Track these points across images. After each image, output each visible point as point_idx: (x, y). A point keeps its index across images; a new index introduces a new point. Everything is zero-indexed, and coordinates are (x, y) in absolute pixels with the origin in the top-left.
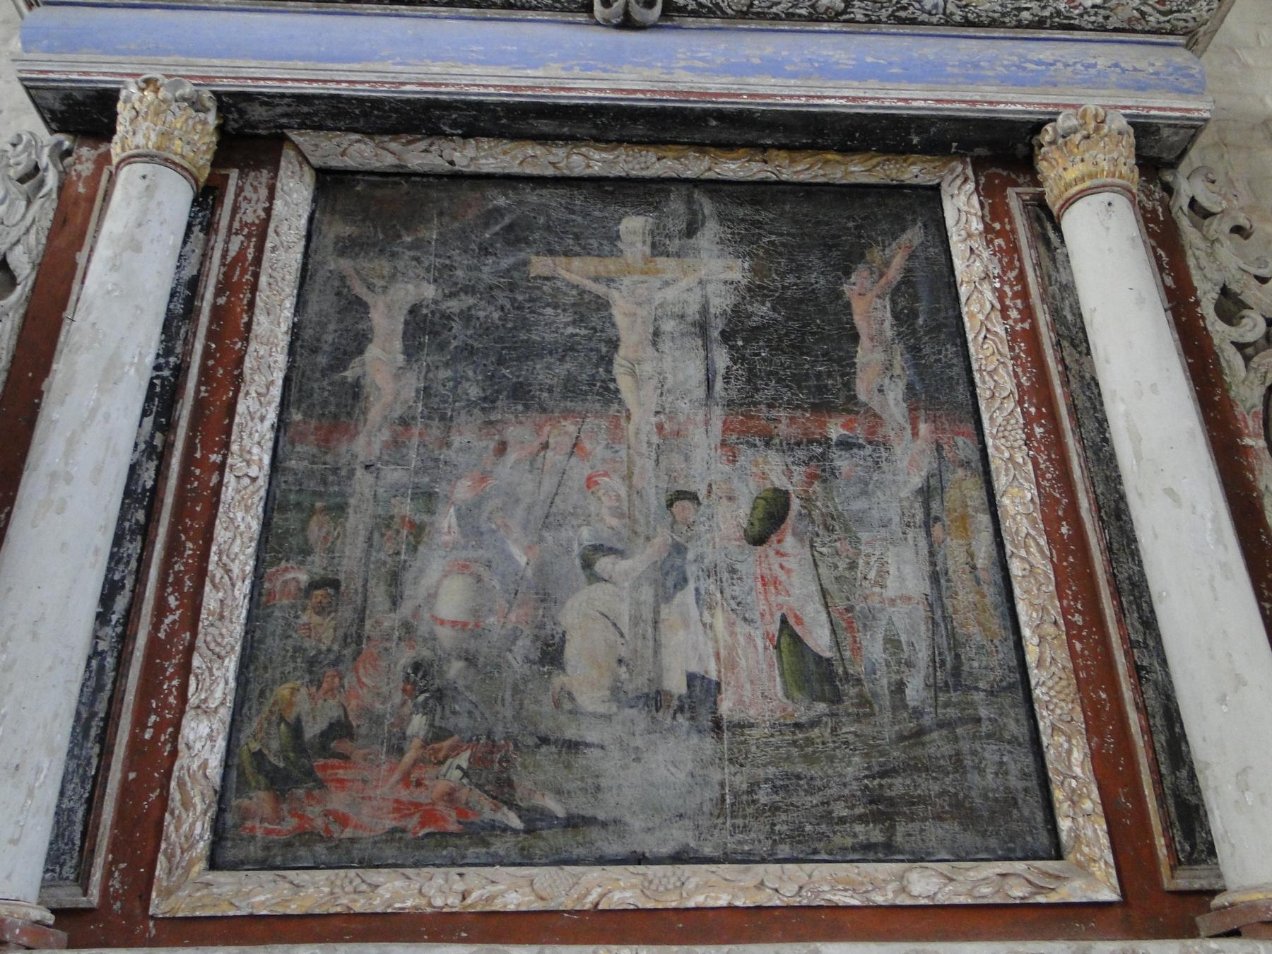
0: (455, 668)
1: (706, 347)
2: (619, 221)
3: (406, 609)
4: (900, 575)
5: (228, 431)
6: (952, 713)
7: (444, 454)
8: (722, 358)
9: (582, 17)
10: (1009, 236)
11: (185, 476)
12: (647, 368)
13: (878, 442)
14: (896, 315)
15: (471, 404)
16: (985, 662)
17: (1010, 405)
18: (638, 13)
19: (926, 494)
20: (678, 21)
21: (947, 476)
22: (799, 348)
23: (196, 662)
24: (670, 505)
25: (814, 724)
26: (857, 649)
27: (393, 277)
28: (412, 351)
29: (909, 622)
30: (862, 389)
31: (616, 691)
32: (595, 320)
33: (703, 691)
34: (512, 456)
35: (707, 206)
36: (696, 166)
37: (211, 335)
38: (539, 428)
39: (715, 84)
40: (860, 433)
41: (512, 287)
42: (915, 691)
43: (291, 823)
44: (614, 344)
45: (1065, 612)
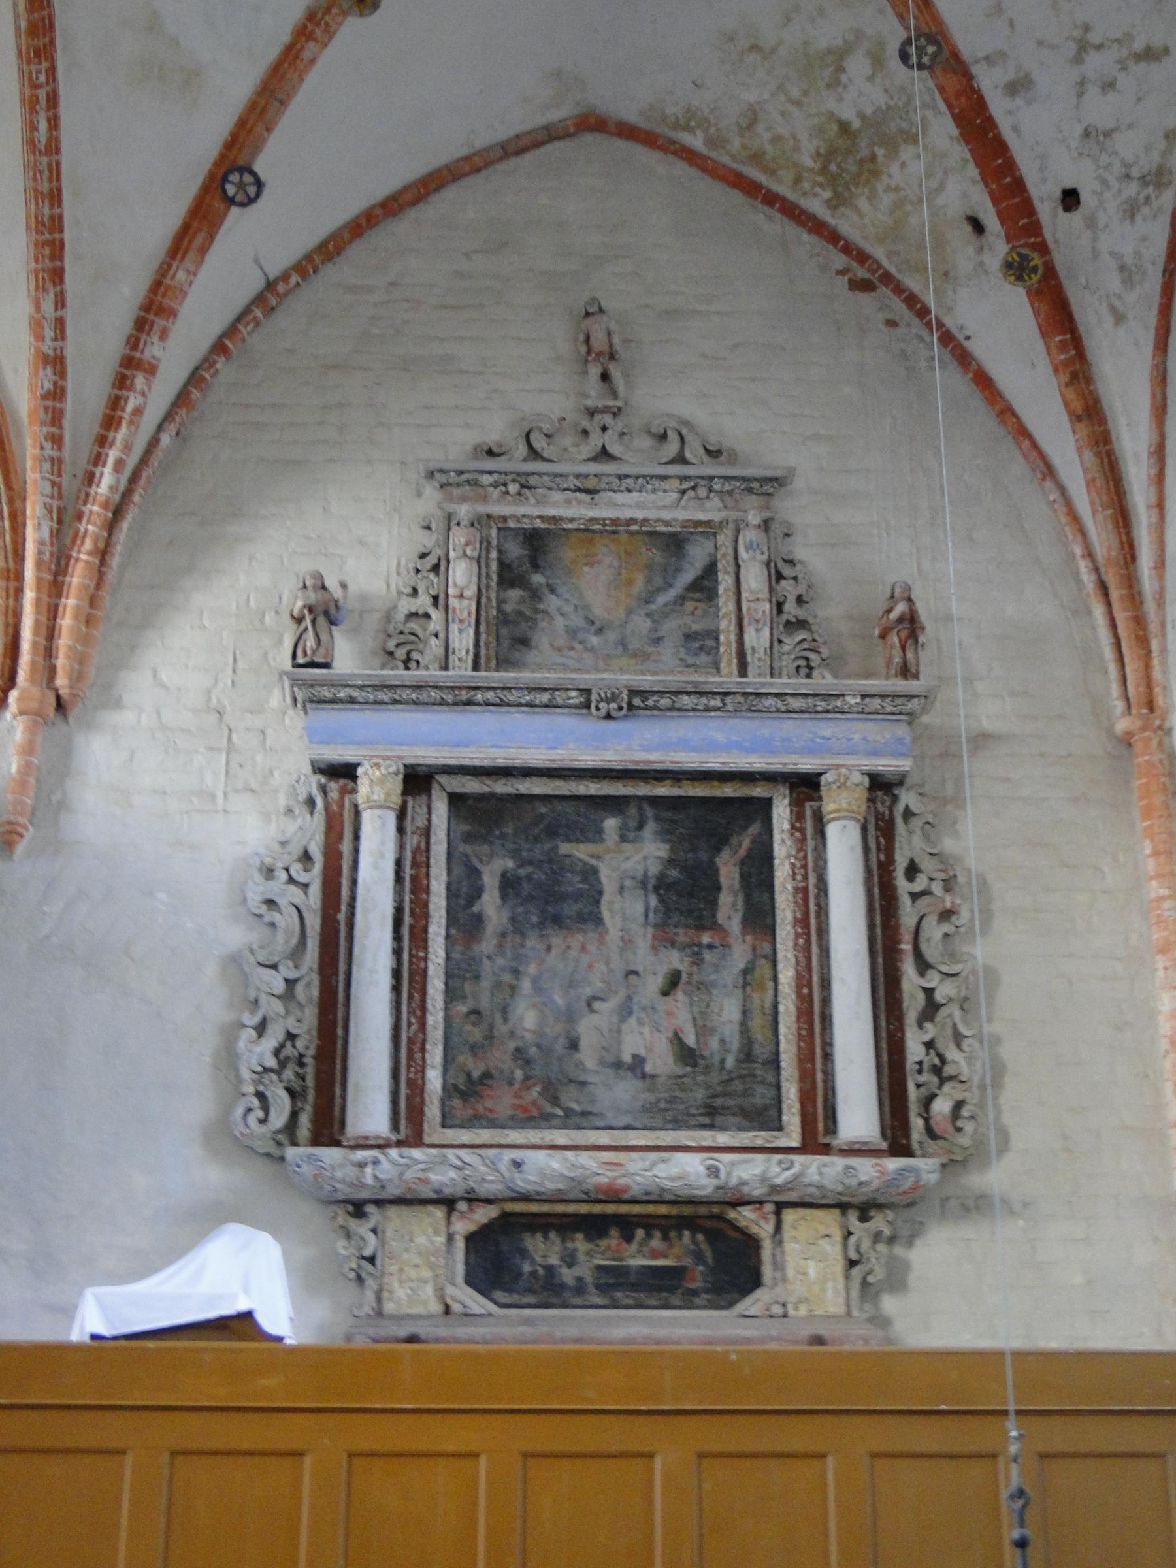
0: (533, 1051)
1: (646, 896)
2: (602, 821)
3: (510, 1024)
4: (728, 1011)
5: (426, 940)
6: (745, 1072)
7: (522, 951)
8: (653, 901)
9: (585, 711)
10: (802, 830)
11: (411, 963)
12: (617, 907)
13: (725, 946)
14: (742, 876)
15: (533, 926)
16: (761, 1051)
17: (789, 928)
18: (614, 714)
19: (746, 972)
20: (635, 712)
21: (758, 963)
22: (691, 895)
23: (428, 1047)
24: (626, 976)
25: (684, 1076)
26: (706, 1044)
27: (492, 856)
28: (504, 897)
30: (721, 917)
31: (602, 1062)
32: (591, 878)
33: (638, 1061)
34: (554, 952)
35: (649, 812)
36: (644, 790)
37: (412, 892)
38: (565, 937)
39: (652, 757)
40: (717, 943)
41: (550, 861)
42: (730, 1063)
43: (471, 1112)
44: (601, 893)
45: (799, 1029)
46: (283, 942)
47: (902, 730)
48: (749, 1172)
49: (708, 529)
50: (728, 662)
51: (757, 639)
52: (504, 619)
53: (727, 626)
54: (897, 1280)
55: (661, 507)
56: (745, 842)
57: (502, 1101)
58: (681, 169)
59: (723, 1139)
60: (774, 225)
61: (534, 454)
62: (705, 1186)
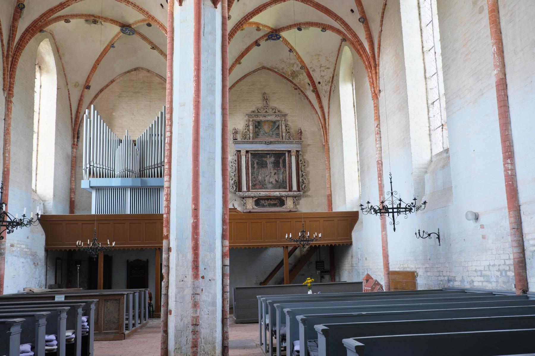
4: (281, 176)
29: (281, 179)
46: (234, 170)
47: (300, 145)
48: (283, 194)
49: (278, 121)
50: (281, 137)
52: (256, 132)
53: (281, 132)
54: (298, 204)
55: (272, 118)
57: (258, 187)
58: (275, 74)
60: (285, 81)
61: (258, 112)
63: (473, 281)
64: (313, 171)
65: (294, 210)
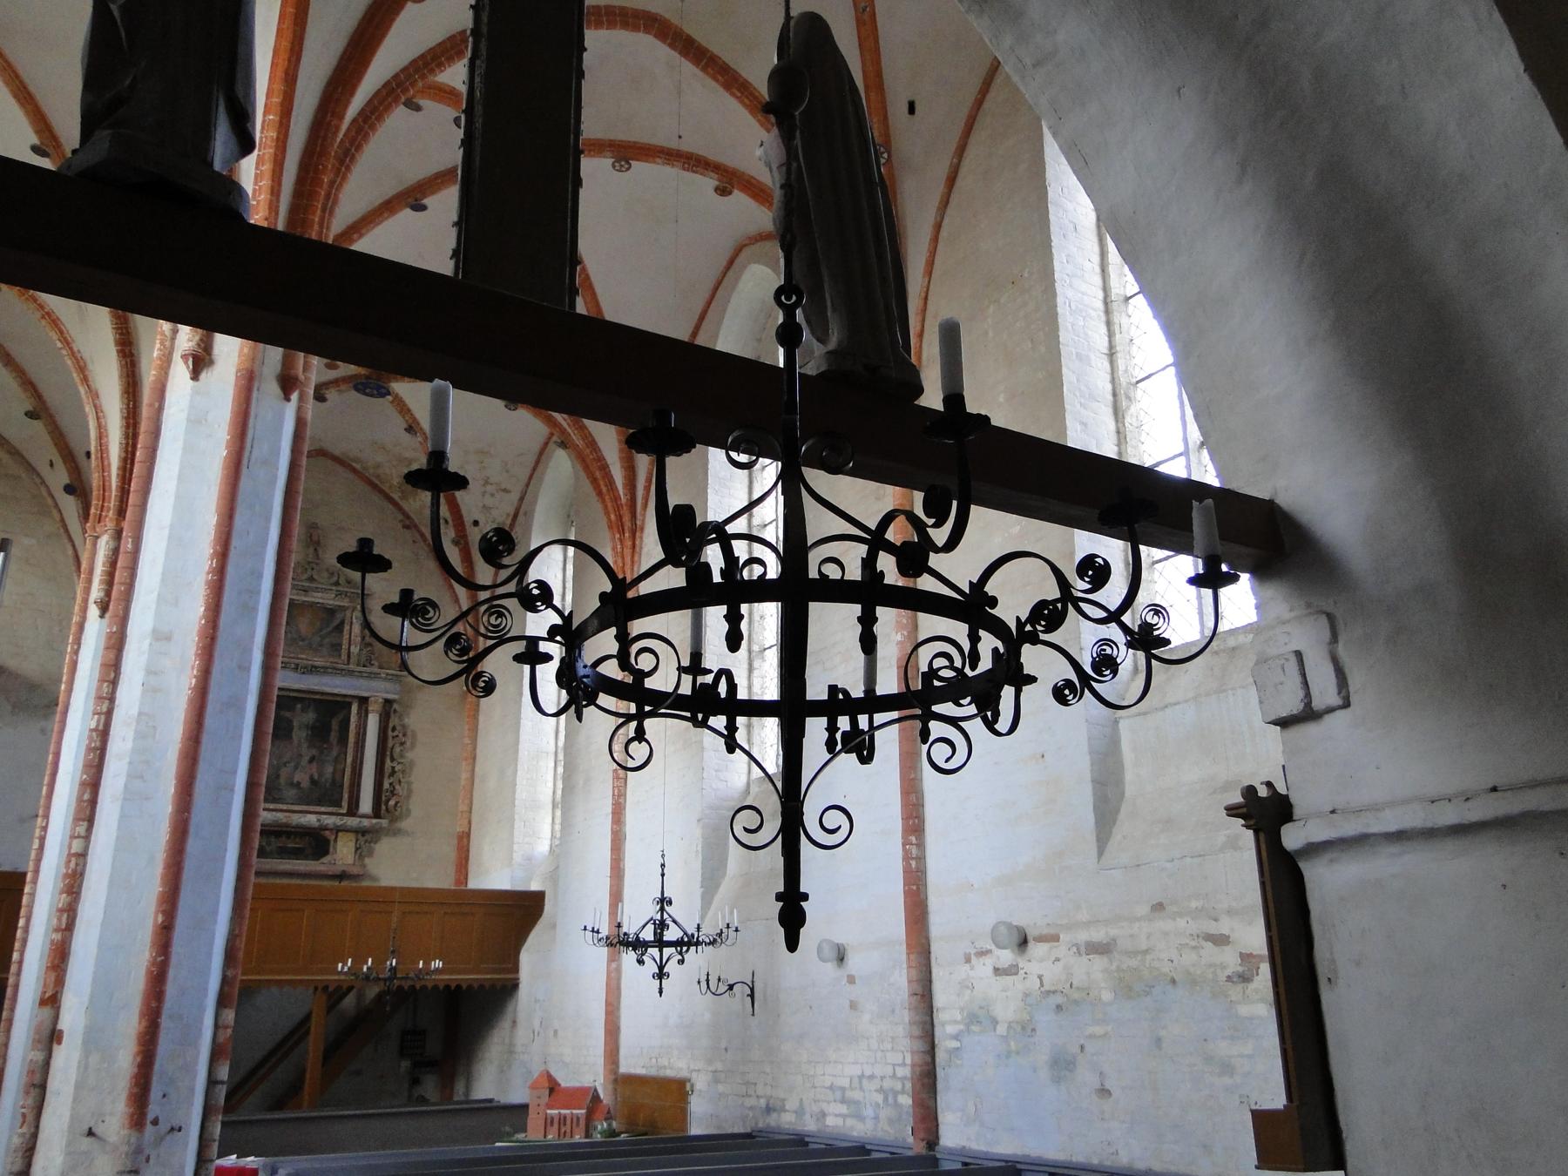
4: (329, 769)
33: (299, 783)
47: (398, 687)
48: (330, 821)
49: (343, 609)
50: (344, 657)
51: (355, 650)
53: (345, 642)
56: (341, 716)
59: (323, 809)
62: (317, 824)
63: (824, 1115)
64: (425, 762)
65: (355, 870)
